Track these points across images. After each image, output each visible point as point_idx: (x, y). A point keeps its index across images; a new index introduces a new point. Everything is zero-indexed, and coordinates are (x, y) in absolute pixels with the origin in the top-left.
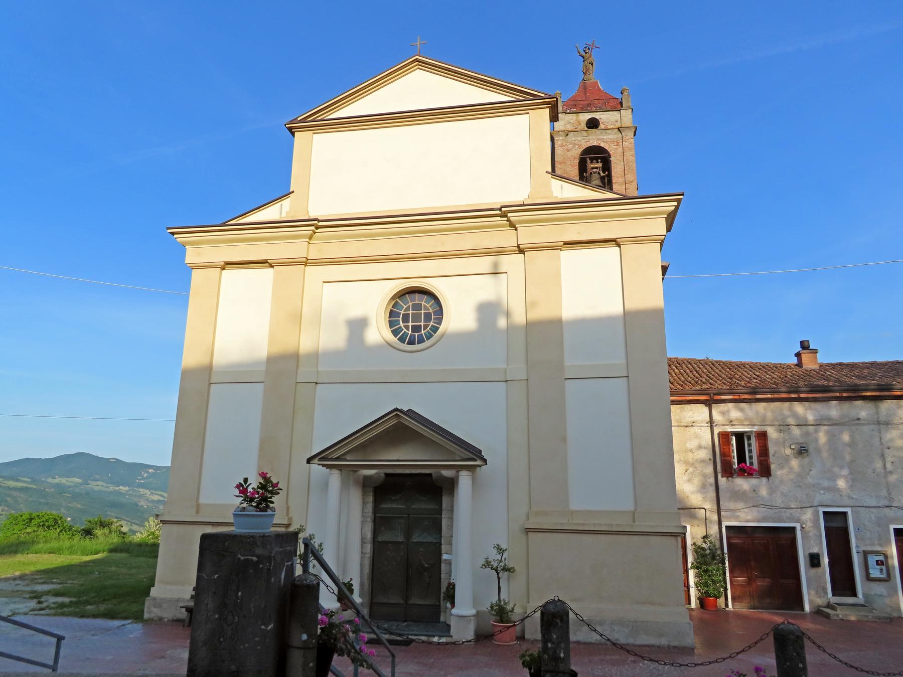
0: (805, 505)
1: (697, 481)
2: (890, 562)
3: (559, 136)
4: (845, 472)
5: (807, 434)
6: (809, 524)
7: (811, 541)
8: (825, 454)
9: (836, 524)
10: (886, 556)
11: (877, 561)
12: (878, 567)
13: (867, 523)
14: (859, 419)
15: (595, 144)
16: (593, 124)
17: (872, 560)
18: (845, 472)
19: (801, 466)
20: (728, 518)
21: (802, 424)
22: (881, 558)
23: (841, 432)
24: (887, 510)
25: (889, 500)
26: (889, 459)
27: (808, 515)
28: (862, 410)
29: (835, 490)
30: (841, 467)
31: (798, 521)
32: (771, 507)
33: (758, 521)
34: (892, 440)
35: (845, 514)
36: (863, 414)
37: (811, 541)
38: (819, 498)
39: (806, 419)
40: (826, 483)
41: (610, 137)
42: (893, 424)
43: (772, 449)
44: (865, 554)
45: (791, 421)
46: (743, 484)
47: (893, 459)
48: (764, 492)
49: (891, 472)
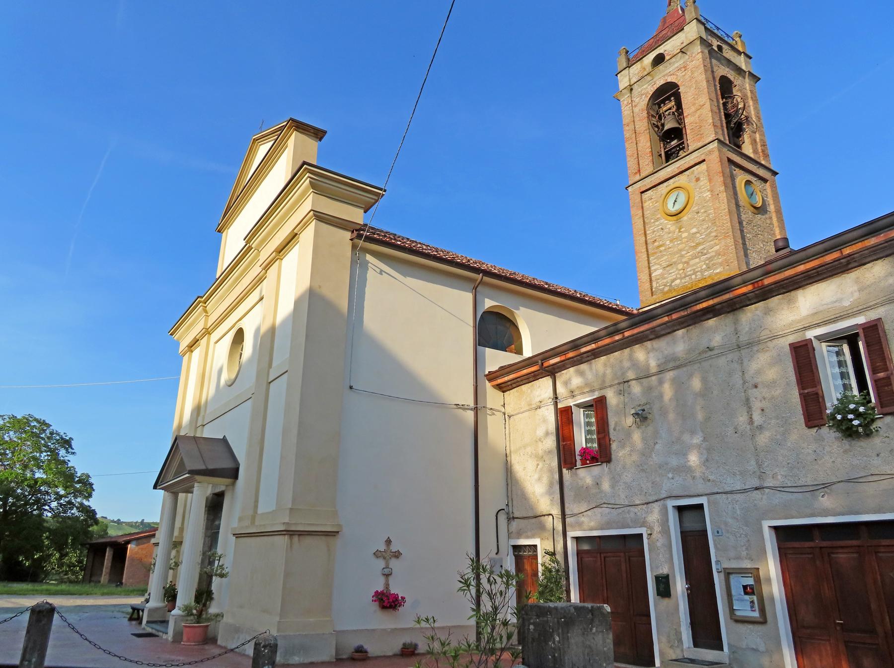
0: (651, 499)
1: (545, 480)
2: (765, 589)
3: (623, 95)
4: (697, 440)
5: (650, 389)
6: (657, 529)
7: (664, 558)
8: (671, 416)
9: (692, 524)
10: (758, 579)
11: (745, 587)
12: (747, 597)
13: (730, 520)
14: (710, 349)
15: (662, 82)
16: (660, 60)
17: (738, 583)
18: (697, 440)
19: (644, 439)
20: (574, 527)
21: (644, 376)
22: (750, 581)
23: (690, 376)
24: (756, 494)
25: (760, 477)
26: (757, 405)
27: (654, 516)
28: (716, 332)
29: (685, 469)
30: (693, 433)
31: (643, 524)
32: (614, 506)
33: (602, 529)
34: (759, 372)
35: (700, 507)
36: (717, 340)
37: (664, 558)
38: (669, 485)
39: (648, 367)
40: (674, 462)
41: (676, 65)
42: (759, 342)
43: (612, 421)
44: (728, 574)
45: (631, 375)
46: (586, 475)
47: (764, 404)
48: (606, 486)
49: (760, 428)
